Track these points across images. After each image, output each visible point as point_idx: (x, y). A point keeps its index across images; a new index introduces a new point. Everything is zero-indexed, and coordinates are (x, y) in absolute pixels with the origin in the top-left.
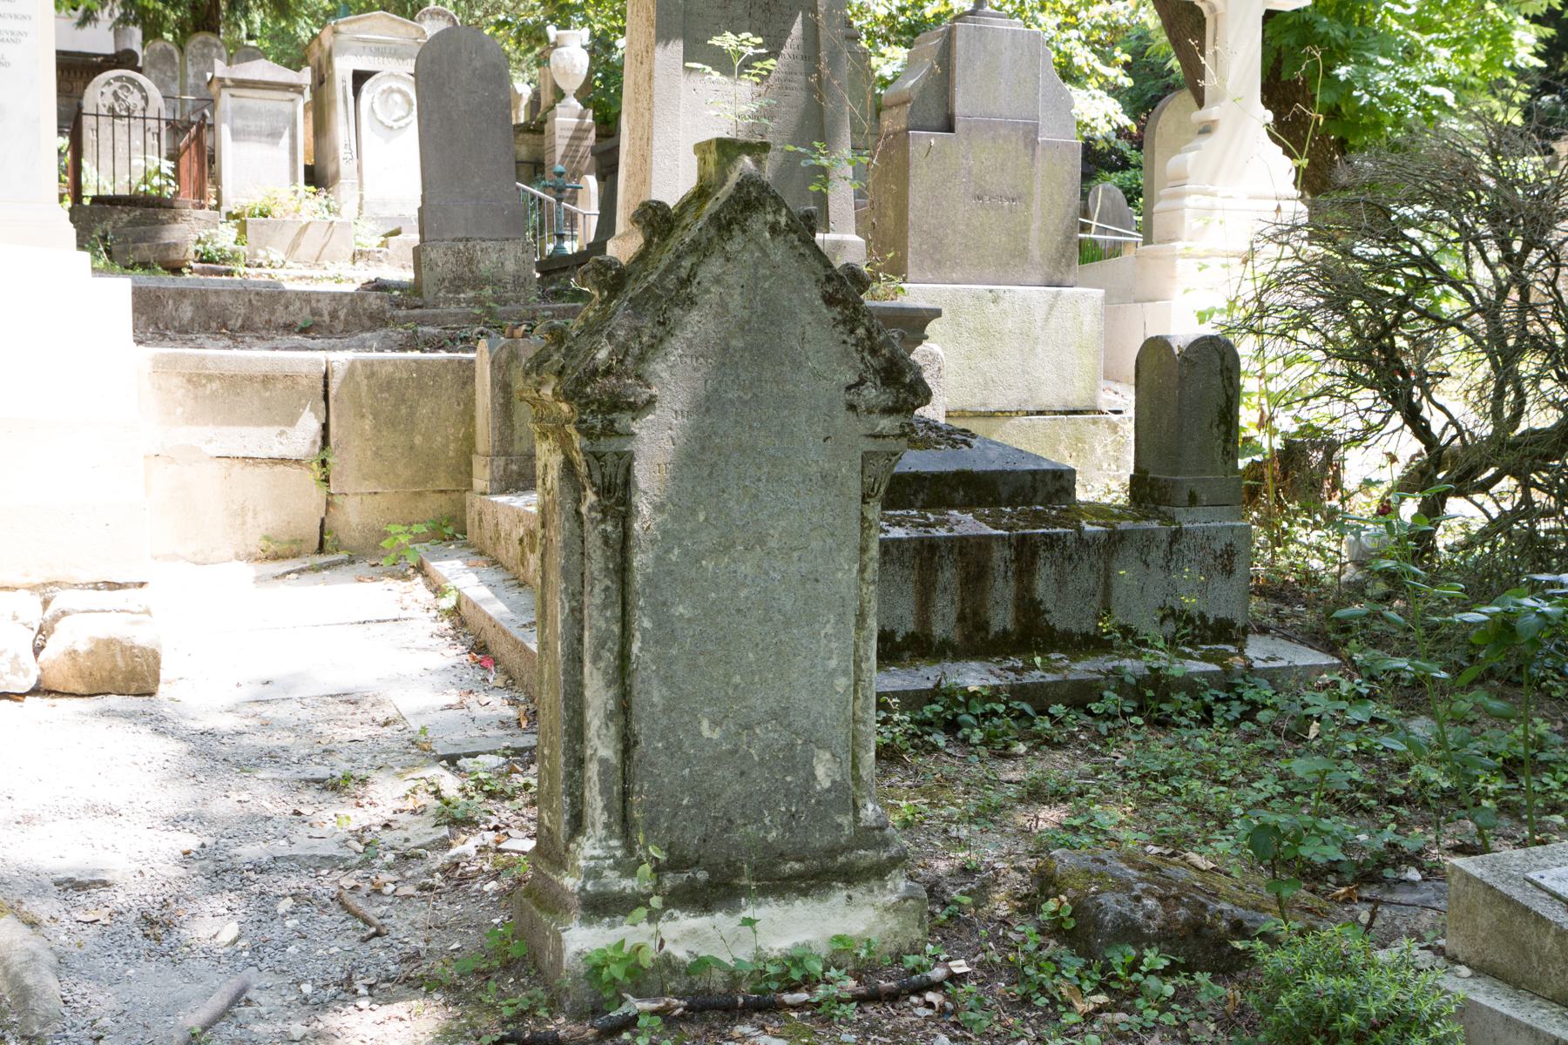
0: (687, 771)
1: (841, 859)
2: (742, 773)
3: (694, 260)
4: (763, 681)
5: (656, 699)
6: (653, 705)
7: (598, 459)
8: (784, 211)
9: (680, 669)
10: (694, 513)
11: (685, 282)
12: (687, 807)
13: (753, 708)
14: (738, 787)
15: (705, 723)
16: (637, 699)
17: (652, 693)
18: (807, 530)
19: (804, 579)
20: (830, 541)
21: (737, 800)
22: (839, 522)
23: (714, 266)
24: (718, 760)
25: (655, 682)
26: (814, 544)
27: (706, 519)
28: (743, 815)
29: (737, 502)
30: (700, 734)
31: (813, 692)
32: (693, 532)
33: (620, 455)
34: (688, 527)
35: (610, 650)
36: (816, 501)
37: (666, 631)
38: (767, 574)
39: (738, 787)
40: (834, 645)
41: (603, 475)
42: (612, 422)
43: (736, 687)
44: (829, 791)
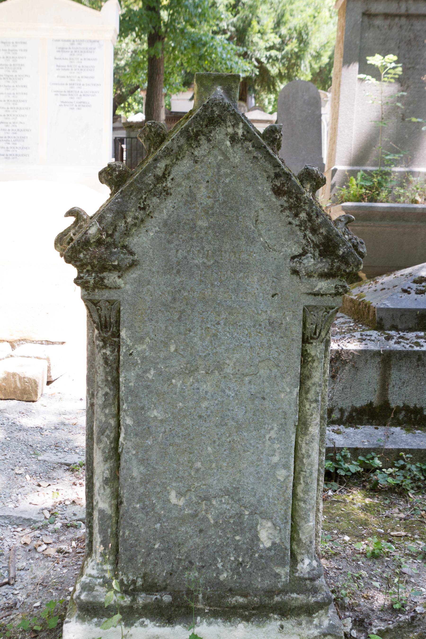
0: (158, 526)
1: (277, 599)
2: (201, 531)
3: (168, 162)
4: (219, 468)
5: (135, 473)
6: (132, 478)
7: (95, 305)
8: (241, 125)
9: (154, 455)
10: (166, 345)
12: (158, 550)
13: (210, 486)
14: (197, 540)
15: (173, 494)
16: (123, 473)
17: (133, 470)
18: (256, 361)
19: (253, 397)
20: (275, 370)
21: (196, 549)
22: (283, 357)
24: (183, 520)
25: (134, 462)
26: (262, 372)
27: (176, 350)
28: (201, 559)
29: (201, 339)
30: (169, 501)
31: (259, 478)
32: (165, 359)
33: (111, 302)
34: (162, 355)
35: (108, 437)
36: (264, 340)
37: (144, 428)
38: (224, 391)
39: (197, 540)
40: (276, 446)
41: (100, 317)
42: (102, 279)
43: (198, 470)
44: (269, 549)
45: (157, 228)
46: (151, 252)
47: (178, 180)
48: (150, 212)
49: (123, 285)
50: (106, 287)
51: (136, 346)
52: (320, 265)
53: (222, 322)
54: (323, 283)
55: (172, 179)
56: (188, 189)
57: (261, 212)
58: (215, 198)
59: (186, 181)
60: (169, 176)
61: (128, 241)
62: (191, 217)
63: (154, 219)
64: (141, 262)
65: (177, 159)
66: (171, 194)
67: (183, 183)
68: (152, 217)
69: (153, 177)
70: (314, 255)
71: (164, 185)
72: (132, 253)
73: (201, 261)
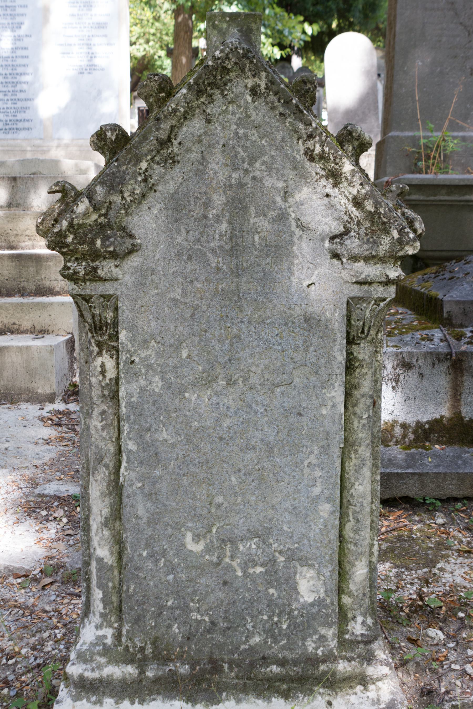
0: (171, 577)
1: (322, 667)
2: (225, 583)
4: (246, 503)
5: (141, 512)
6: (137, 517)
7: (87, 301)
8: (263, 74)
9: (164, 487)
10: (177, 349)
11: (165, 143)
12: (171, 608)
13: (236, 526)
14: (221, 595)
15: (189, 537)
16: (126, 511)
17: (139, 508)
18: (290, 368)
19: (287, 413)
20: (313, 378)
21: (220, 606)
22: (323, 361)
23: (195, 125)
24: (202, 569)
25: (140, 498)
26: (297, 381)
27: (189, 356)
28: (226, 619)
29: (219, 341)
30: (184, 545)
31: (297, 515)
32: (176, 367)
33: (107, 297)
34: (171, 362)
35: (106, 466)
36: (299, 341)
37: (152, 455)
38: (250, 407)
39: (221, 595)
40: (318, 473)
41: (93, 316)
42: (95, 269)
43: (219, 506)
44: (312, 605)
45: (162, 205)
46: (155, 234)
47: (188, 144)
48: (153, 185)
49: (120, 276)
51: (139, 352)
52: (366, 247)
53: (246, 320)
54: (371, 269)
55: (180, 143)
56: (199, 155)
57: (290, 182)
58: (234, 165)
59: (197, 146)
60: (175, 139)
61: (126, 221)
62: (204, 189)
63: (158, 193)
64: (143, 246)
65: (185, 118)
66: (179, 162)
67: (193, 148)
68: (155, 191)
69: (155, 142)
70: (359, 234)
71: (169, 151)
72: (131, 236)
73: (217, 245)
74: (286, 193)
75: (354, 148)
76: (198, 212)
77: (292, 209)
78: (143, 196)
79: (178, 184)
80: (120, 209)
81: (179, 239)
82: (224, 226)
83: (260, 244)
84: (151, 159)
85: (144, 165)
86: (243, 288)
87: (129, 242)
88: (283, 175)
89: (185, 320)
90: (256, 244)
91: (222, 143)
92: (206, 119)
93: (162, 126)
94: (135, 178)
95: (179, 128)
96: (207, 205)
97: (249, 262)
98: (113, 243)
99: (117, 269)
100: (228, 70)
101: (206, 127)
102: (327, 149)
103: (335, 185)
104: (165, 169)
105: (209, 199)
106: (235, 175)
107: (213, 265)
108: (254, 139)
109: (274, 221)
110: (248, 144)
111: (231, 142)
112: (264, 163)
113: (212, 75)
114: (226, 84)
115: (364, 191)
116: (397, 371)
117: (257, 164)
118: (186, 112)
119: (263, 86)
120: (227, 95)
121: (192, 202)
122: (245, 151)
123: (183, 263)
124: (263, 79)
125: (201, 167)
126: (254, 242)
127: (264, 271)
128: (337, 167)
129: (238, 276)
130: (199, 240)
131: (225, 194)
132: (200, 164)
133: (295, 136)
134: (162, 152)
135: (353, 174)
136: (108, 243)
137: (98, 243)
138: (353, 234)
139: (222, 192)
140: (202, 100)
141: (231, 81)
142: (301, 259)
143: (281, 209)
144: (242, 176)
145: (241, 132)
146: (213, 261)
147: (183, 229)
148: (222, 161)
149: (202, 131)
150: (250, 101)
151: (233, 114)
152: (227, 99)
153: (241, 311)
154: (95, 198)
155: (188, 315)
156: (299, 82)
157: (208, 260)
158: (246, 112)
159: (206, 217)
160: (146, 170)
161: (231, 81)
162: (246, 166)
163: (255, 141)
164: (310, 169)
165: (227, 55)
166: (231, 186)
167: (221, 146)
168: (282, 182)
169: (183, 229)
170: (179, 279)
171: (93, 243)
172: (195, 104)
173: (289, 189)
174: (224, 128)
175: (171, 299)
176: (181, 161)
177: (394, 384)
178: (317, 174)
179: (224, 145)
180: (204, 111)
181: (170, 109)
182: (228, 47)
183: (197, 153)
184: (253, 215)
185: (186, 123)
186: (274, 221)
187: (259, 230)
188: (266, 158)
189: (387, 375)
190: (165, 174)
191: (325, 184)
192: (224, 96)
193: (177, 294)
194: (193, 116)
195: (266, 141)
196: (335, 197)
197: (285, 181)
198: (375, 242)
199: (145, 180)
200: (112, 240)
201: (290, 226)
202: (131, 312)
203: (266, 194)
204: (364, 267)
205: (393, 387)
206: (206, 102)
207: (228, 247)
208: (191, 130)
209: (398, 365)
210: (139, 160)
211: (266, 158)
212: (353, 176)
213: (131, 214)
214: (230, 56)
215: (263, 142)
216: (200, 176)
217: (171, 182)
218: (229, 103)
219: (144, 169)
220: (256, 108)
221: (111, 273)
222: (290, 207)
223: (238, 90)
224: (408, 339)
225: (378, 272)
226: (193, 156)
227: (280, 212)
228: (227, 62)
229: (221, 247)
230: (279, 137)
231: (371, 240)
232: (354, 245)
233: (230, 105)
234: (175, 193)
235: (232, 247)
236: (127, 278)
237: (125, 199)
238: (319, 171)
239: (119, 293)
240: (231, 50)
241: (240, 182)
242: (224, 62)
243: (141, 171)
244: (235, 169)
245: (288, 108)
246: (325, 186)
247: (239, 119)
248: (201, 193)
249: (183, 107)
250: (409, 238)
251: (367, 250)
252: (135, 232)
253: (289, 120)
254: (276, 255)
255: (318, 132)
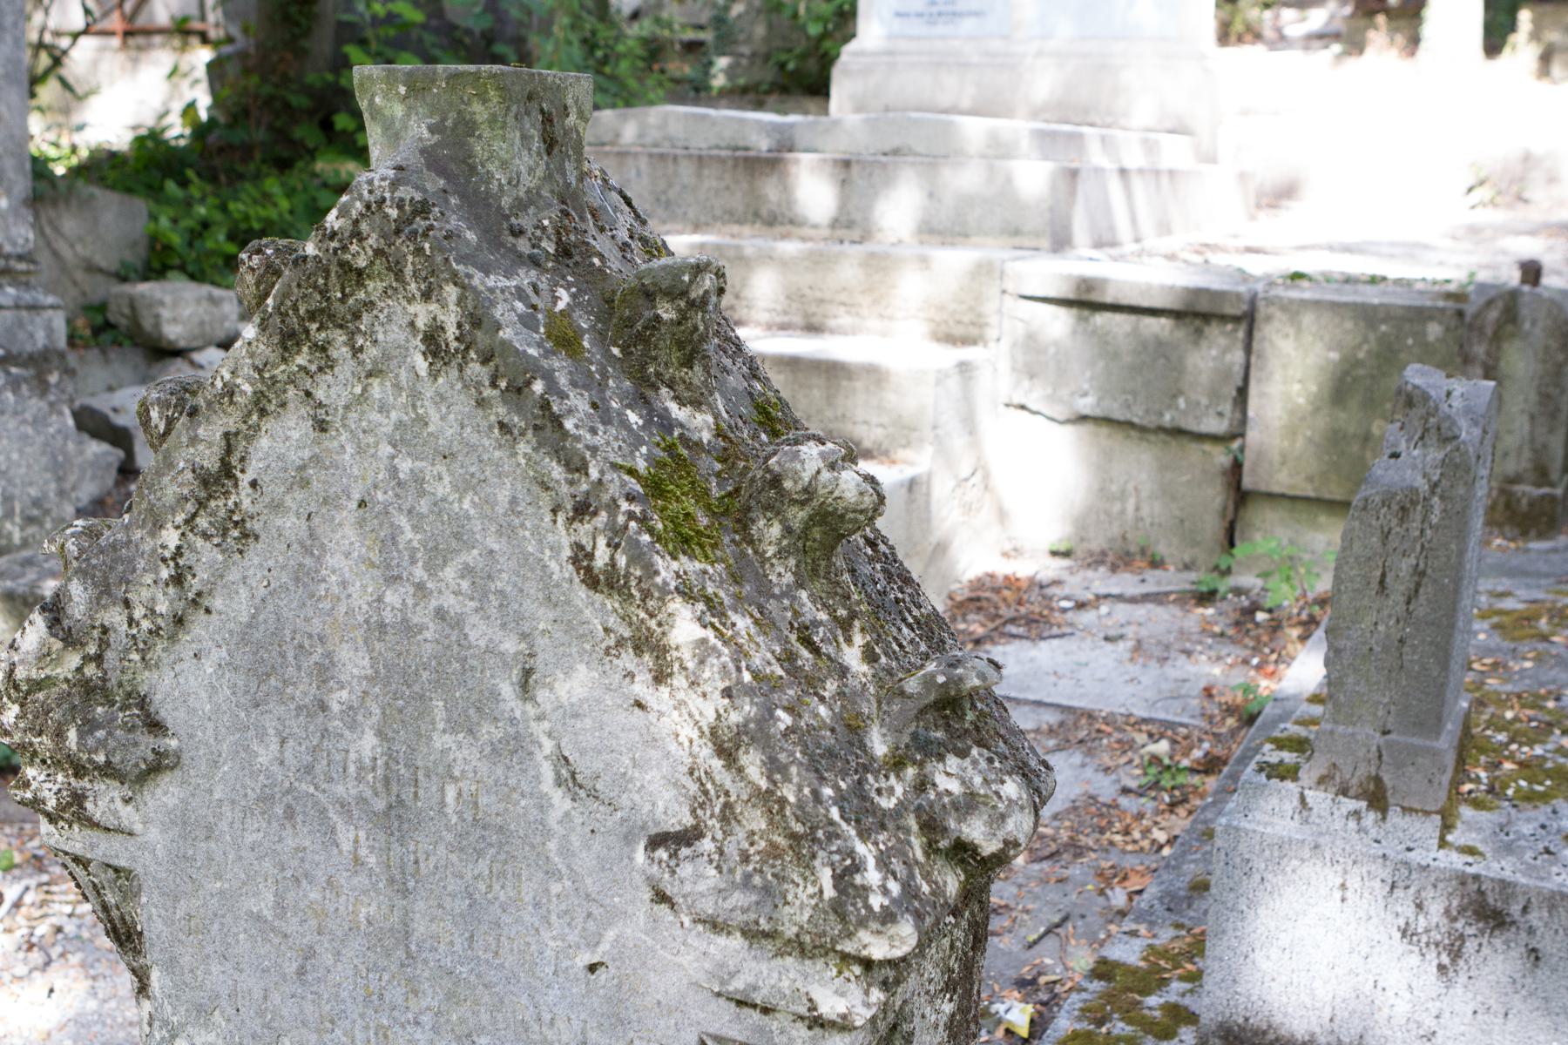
8: (451, 292)
42: (78, 798)
46: (210, 732)
47: (273, 490)
48: (199, 594)
49: (138, 828)
50: (93, 824)
51: (190, 1029)
52: (739, 899)
53: (426, 1019)
54: (764, 967)
55: (254, 484)
56: (304, 525)
57: (541, 642)
58: (388, 567)
59: (299, 495)
61: (147, 681)
63: (214, 616)
64: (185, 758)
65: (263, 413)
69: (189, 475)
70: (721, 852)
72: (155, 726)
73: (353, 792)
74: (527, 673)
75: (788, 530)
76: (305, 690)
77: (546, 725)
78: (179, 621)
79: (257, 601)
80: (127, 650)
81: (265, 755)
82: (367, 744)
83: (460, 814)
84: (187, 522)
85: (171, 538)
86: (420, 928)
87: (147, 743)
88: (520, 618)
89: (284, 977)
90: (449, 810)
91: (357, 496)
92: (314, 418)
93: (201, 431)
94: (156, 571)
95: (249, 439)
96: (325, 672)
97: (433, 860)
98: (102, 743)
99: (129, 808)
100: (360, 272)
101: (317, 442)
102: (622, 561)
103: (660, 677)
104: (223, 552)
105: (329, 655)
106: (391, 597)
107: (346, 846)
108: (440, 492)
109: (495, 752)
110: (424, 506)
111: (380, 496)
112: (467, 571)
113: (315, 287)
114: (357, 316)
115: (735, 718)
116: (1459, 925)
117: (449, 573)
118: (259, 397)
119: (451, 331)
120: (361, 350)
121: (290, 655)
122: (416, 529)
123: (275, 824)
124: (452, 307)
125: (308, 561)
126: (443, 803)
127: (470, 896)
128: (653, 623)
129: (405, 893)
130: (309, 769)
131: (371, 651)
132: (308, 551)
133: (546, 501)
134: (213, 504)
135: (703, 651)
136: (90, 742)
137: (72, 735)
138: (707, 845)
139: (360, 642)
140: (301, 360)
141: (369, 305)
142: (568, 883)
143: (512, 721)
144: (410, 602)
145: (405, 466)
146: (345, 836)
147: (271, 731)
148: (359, 550)
149: (306, 454)
150: (423, 373)
151: (383, 409)
152: (361, 363)
153: (415, 993)
154: (69, 612)
155: (291, 968)
156: (632, 290)
157: (333, 830)
158: (414, 406)
159: (323, 707)
160: (179, 551)
161: (369, 305)
162: (419, 573)
163: (444, 500)
164: (588, 613)
165: (356, 222)
166: (382, 626)
167: (354, 505)
168: (514, 638)
169: (271, 731)
170: (267, 864)
171: (59, 735)
172: (280, 371)
173: (539, 663)
174: (361, 450)
175: (250, 914)
176: (263, 536)
177: (1445, 959)
178: (607, 630)
179: (362, 504)
180: (308, 394)
181: (219, 384)
182: (360, 197)
183: (298, 515)
184: (441, 726)
185: (268, 424)
186: (495, 752)
187: (457, 773)
188: (472, 557)
189: (1427, 931)
190: (227, 568)
191: (631, 667)
192: (357, 351)
193: (264, 903)
194: (283, 405)
195: (472, 502)
196: (661, 714)
197: (524, 636)
198: (766, 889)
199: (178, 580)
200: (100, 734)
201: (538, 778)
202: (165, 924)
203: (472, 669)
204: (744, 954)
205: (1442, 968)
206: (313, 368)
207: (380, 805)
208: (281, 448)
209: (1462, 910)
210: (158, 526)
211: (472, 557)
212: (702, 662)
213: (157, 666)
214: (364, 227)
215: (466, 505)
216: (305, 585)
217: (244, 593)
218: (370, 375)
219: (172, 547)
220: (441, 398)
221: (115, 813)
222: (540, 718)
223: (391, 337)
224: (1527, 829)
225: (785, 984)
226: (290, 524)
227: (512, 731)
228: (354, 248)
229: (362, 800)
230: (503, 496)
231: (757, 880)
232: (702, 887)
233: (375, 382)
234: (249, 625)
235: (390, 807)
236: (154, 834)
237: (138, 625)
238: (612, 621)
239: (139, 870)
240: (368, 207)
241: (405, 620)
242: (345, 248)
243: (167, 554)
244: (393, 580)
245: (519, 410)
246: (630, 675)
247: (400, 425)
248: (310, 636)
249: (249, 380)
250: (868, 907)
251: (745, 911)
252: (166, 714)
253: (523, 447)
254: (503, 856)
255: (605, 498)
